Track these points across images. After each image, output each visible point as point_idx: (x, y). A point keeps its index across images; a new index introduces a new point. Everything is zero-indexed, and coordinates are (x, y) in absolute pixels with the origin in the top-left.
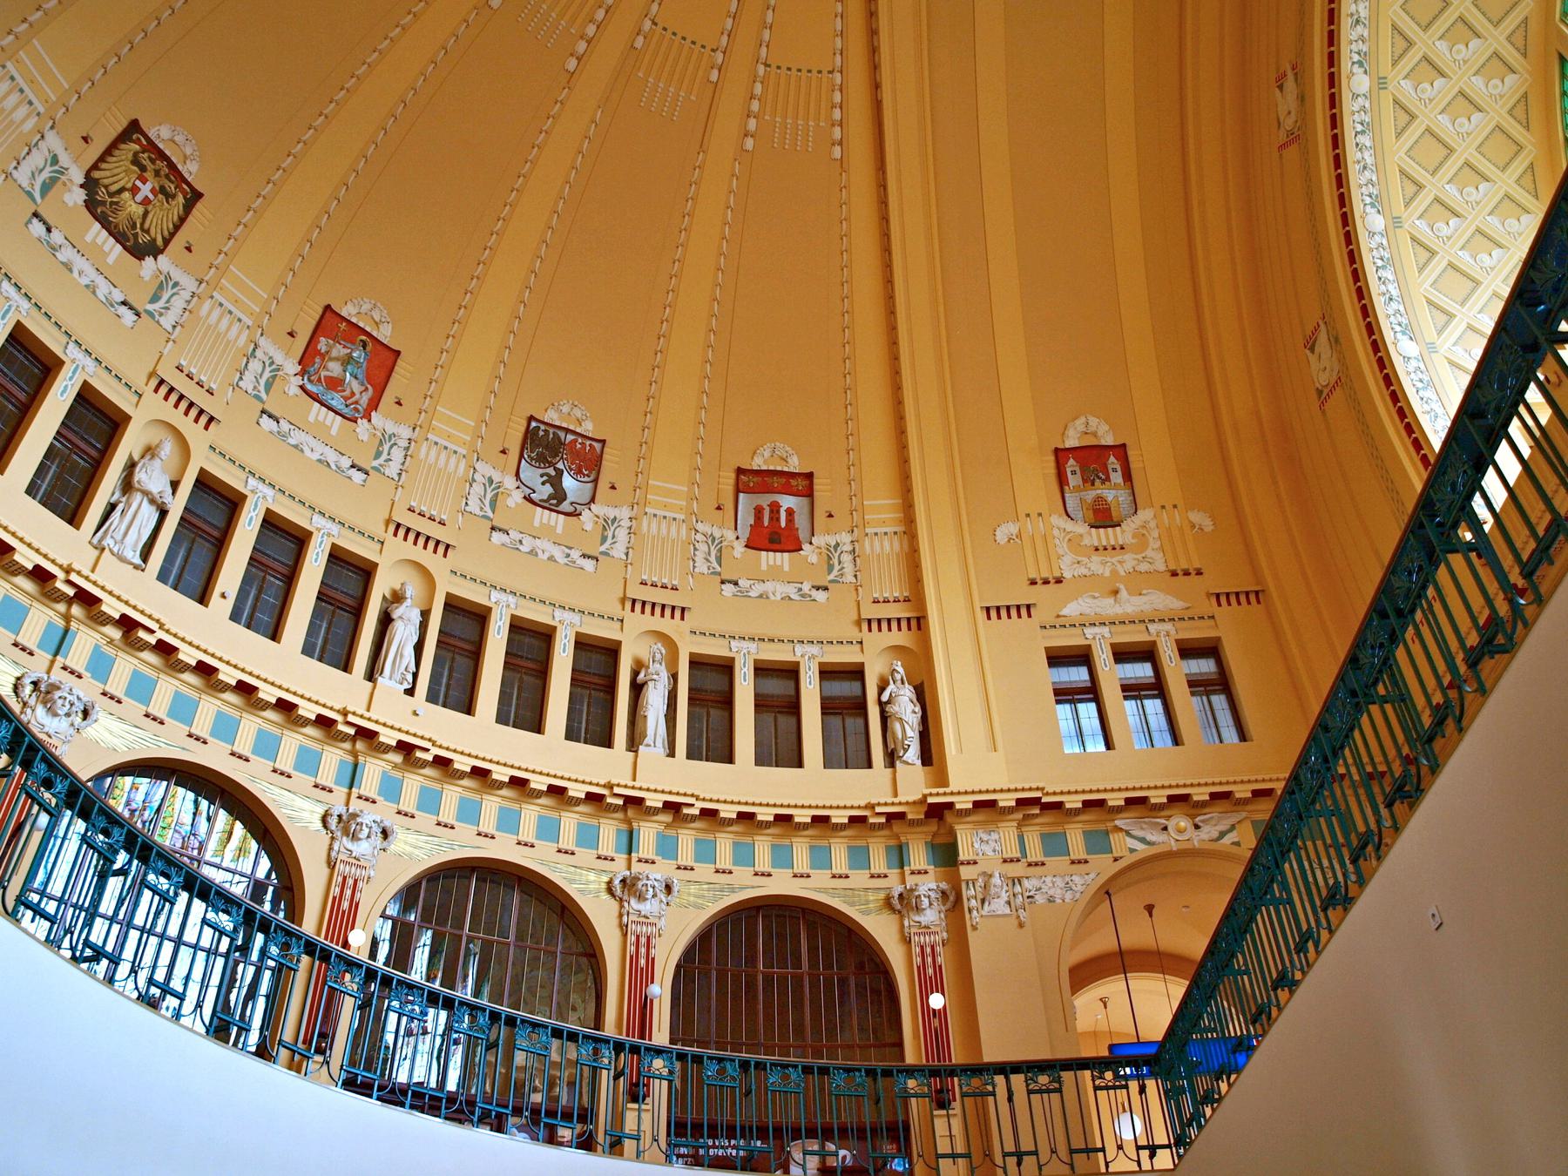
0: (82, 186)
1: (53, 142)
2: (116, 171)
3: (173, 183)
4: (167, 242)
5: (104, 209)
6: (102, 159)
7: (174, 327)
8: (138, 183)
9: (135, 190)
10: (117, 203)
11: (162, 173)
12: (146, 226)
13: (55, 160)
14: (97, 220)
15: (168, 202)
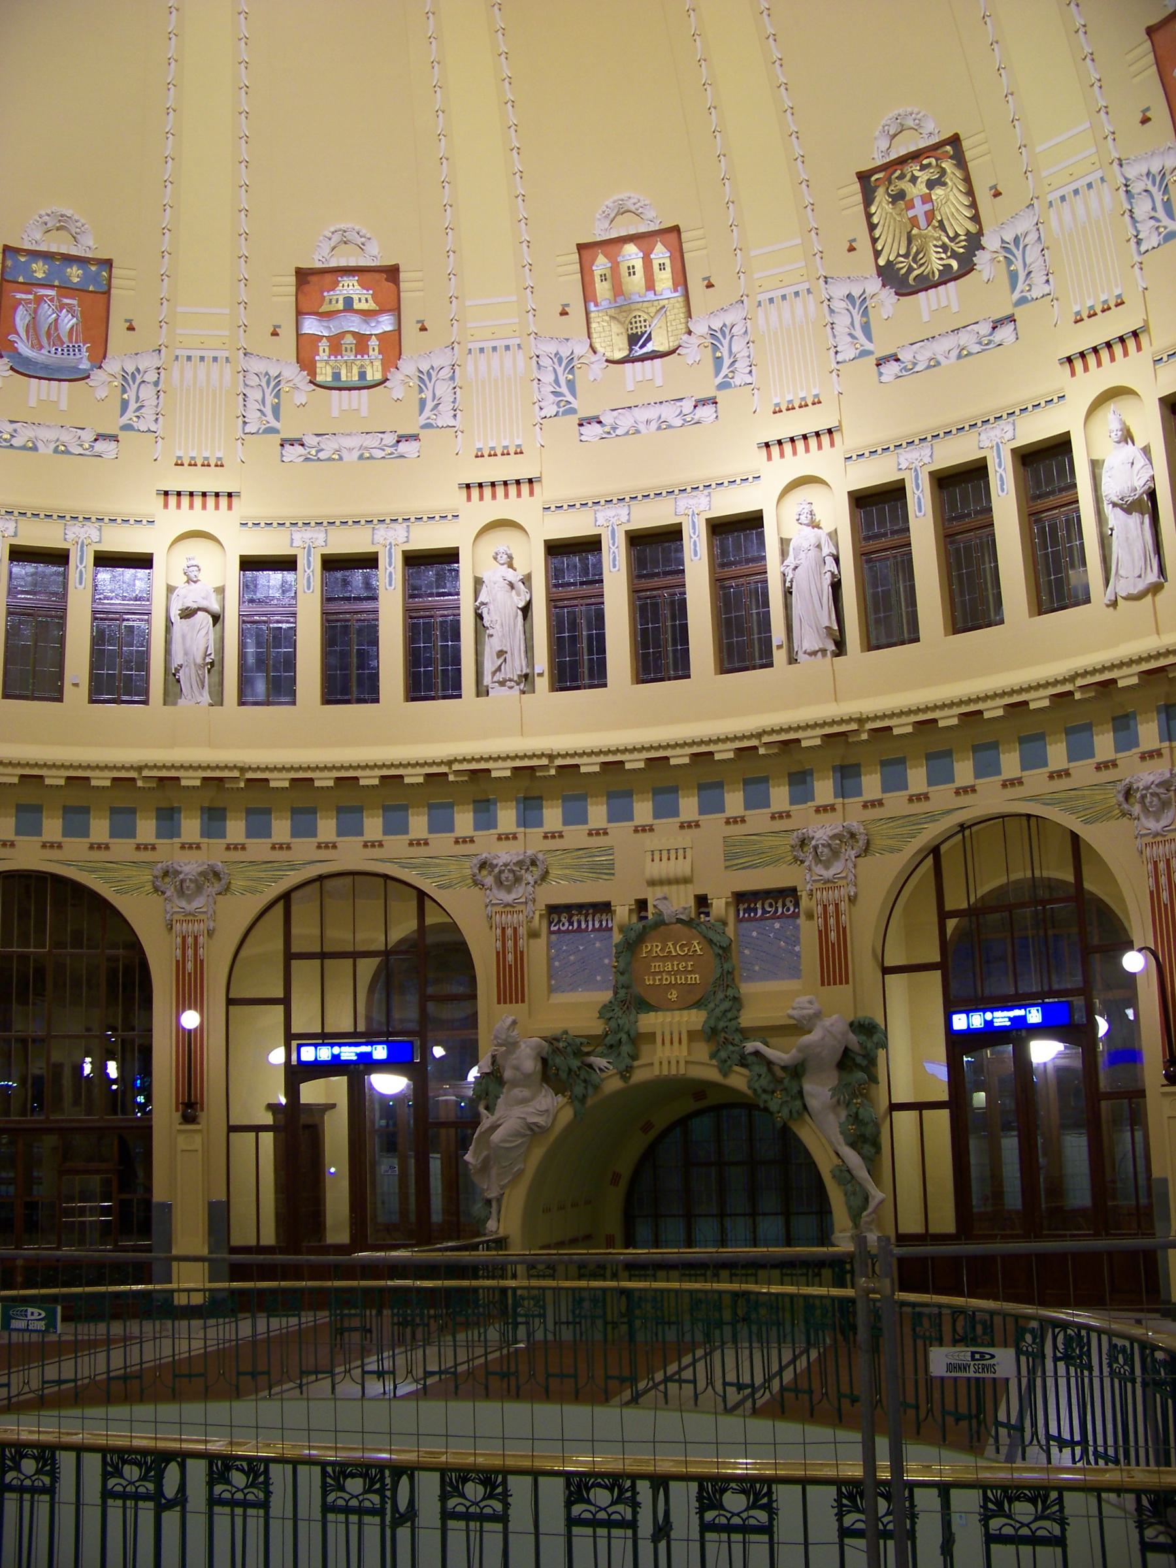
0: (884, 286)
1: (839, 291)
2: (891, 228)
3: (929, 165)
4: (976, 219)
5: (916, 273)
6: (874, 241)
7: (1047, 281)
8: (911, 213)
9: (914, 222)
10: (917, 253)
11: (917, 173)
12: (951, 234)
13: (849, 296)
14: (916, 292)
15: (944, 184)
